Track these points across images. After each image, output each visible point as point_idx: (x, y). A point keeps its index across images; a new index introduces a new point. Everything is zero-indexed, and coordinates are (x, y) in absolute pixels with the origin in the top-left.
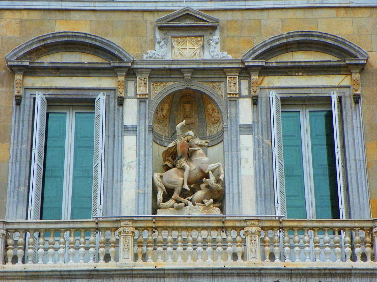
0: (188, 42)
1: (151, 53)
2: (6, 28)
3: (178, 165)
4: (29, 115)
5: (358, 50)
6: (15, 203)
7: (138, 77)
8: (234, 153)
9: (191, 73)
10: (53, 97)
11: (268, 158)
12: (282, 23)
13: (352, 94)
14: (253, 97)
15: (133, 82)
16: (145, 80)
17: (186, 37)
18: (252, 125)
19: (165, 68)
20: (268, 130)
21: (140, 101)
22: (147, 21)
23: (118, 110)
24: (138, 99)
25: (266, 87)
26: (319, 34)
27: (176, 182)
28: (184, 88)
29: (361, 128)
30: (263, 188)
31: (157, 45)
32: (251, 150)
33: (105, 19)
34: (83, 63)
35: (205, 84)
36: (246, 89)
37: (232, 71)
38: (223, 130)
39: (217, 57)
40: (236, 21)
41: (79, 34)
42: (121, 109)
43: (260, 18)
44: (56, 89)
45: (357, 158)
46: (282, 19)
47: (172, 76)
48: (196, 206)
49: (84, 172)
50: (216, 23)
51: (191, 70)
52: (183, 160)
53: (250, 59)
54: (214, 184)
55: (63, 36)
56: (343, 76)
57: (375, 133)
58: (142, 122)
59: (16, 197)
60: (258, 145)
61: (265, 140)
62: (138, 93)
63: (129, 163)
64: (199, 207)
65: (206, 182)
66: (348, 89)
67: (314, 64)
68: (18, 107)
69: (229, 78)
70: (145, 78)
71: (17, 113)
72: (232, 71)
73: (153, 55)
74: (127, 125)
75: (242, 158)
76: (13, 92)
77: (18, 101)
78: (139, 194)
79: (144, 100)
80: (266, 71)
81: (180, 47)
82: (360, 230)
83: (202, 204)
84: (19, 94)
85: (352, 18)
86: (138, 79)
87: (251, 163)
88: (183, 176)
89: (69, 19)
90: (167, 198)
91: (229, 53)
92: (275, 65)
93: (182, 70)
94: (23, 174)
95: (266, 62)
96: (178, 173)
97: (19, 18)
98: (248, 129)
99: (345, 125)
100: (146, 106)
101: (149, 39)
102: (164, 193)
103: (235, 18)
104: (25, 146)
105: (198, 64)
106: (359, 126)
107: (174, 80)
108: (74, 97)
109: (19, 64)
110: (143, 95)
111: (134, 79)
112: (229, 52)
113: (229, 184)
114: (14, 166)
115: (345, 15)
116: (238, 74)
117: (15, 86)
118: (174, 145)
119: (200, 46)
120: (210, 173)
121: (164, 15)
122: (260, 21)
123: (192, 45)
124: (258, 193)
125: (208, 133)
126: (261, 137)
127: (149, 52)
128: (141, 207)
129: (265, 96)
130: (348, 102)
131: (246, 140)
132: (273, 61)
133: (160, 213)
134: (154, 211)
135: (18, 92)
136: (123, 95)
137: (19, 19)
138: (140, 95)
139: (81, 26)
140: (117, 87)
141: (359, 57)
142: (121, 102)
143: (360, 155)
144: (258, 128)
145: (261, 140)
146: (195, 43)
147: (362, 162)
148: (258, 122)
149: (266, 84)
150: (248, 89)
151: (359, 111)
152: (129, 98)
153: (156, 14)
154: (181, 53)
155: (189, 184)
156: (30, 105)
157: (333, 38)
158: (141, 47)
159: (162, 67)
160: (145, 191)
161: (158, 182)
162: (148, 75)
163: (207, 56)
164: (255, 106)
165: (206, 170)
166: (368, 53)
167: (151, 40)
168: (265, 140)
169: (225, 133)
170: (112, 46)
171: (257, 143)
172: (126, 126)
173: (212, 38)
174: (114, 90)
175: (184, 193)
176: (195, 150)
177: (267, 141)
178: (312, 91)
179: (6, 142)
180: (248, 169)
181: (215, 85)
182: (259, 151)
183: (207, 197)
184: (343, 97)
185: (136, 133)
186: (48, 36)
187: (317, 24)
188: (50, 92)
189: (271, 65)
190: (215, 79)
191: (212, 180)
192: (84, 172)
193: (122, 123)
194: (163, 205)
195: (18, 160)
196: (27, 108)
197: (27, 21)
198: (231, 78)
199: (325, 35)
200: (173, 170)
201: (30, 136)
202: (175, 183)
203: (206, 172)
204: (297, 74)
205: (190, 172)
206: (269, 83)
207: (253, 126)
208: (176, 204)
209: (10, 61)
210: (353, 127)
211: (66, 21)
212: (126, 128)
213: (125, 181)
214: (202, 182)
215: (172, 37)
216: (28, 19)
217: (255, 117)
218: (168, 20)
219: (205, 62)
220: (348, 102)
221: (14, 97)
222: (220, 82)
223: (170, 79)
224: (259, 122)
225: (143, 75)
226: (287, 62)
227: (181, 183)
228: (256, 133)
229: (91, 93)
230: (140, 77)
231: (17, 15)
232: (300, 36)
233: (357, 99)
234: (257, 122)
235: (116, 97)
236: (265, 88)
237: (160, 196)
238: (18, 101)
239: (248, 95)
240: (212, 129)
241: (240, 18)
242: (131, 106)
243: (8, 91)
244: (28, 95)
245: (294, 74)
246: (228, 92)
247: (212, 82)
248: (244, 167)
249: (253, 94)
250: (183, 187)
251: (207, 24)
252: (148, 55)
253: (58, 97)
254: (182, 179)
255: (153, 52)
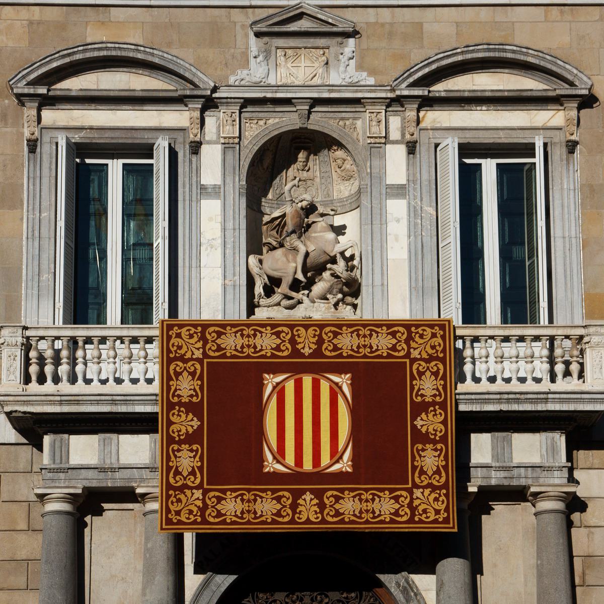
0: (303, 56)
1: (242, 74)
2: (7, 35)
3: (288, 244)
4: (50, 169)
5: (576, 75)
6: (35, 297)
7: (222, 111)
8: (376, 228)
9: (307, 105)
10: (88, 141)
11: (429, 234)
12: (457, 29)
13: (563, 140)
14: (408, 142)
15: (215, 118)
16: (233, 115)
17: (300, 48)
18: (405, 185)
19: (265, 97)
20: (430, 193)
21: (225, 147)
22: (235, 23)
23: (190, 161)
24: (222, 144)
25: (429, 128)
26: (515, 48)
27: (284, 269)
28: (297, 127)
29: (575, 190)
30: (420, 278)
31: (252, 61)
32: (405, 222)
33: (167, 20)
34: (134, 90)
35: (331, 122)
36: (397, 131)
37: (374, 102)
38: (359, 191)
39: (350, 80)
40: (383, 25)
41: (125, 46)
42: (194, 159)
43: (422, 21)
44: (91, 128)
45: (567, 235)
46: (456, 23)
47: (277, 109)
48: (316, 304)
49: (138, 252)
50: (349, 27)
51: (309, 100)
52: (294, 236)
53: (404, 85)
54: (345, 272)
55: (99, 49)
56: (551, 113)
57: (591, 193)
58: (229, 180)
59: (36, 289)
60: (415, 215)
61: (425, 208)
62: (222, 135)
63: (209, 240)
64: (322, 306)
65: (330, 269)
66: (557, 132)
67: (506, 94)
68: (31, 155)
69: (370, 112)
70: (232, 113)
71: (32, 165)
72: (374, 102)
73: (246, 76)
74: (204, 183)
75: (390, 234)
76: (23, 134)
77: (33, 146)
78: (225, 286)
79: (232, 146)
80: (428, 102)
81: (289, 65)
82: (565, 338)
83: (326, 301)
84: (33, 137)
85: (570, 22)
86: (221, 113)
87: (404, 241)
88: (296, 262)
89: (107, 20)
90: (269, 291)
91: (370, 75)
92: (445, 95)
93: (293, 101)
94: (44, 256)
95: (427, 88)
96: (286, 256)
97: (26, 19)
98: (399, 191)
99: (551, 187)
100: (234, 156)
101: (239, 51)
102: (265, 284)
103: (381, 21)
104: (46, 214)
105: (320, 92)
106: (572, 187)
107: (281, 114)
108: (120, 141)
109: (32, 91)
110: (230, 138)
111: (215, 113)
112: (372, 72)
113: (368, 272)
114: (30, 243)
115: (559, 18)
116: (384, 108)
117: (26, 125)
118: (280, 214)
119: (323, 63)
120: (338, 256)
121: (265, 13)
122: (421, 25)
123: (310, 62)
124: (413, 285)
125: (335, 194)
126: (419, 203)
127: (239, 72)
128: (229, 306)
129: (427, 141)
130: (558, 153)
131: (397, 208)
132: (440, 88)
133: (261, 314)
134: (251, 307)
135: (33, 134)
136: (197, 139)
137: (27, 20)
138: (225, 138)
139: (130, 35)
140: (188, 127)
141: (577, 84)
142: (196, 148)
143: (573, 230)
144: (415, 189)
145: (418, 208)
146: (314, 58)
147: (574, 241)
148: (414, 182)
149: (430, 123)
150: (400, 129)
151: (574, 165)
152: (209, 143)
153: (250, 10)
154: (292, 74)
155: (305, 272)
156: (51, 154)
157: (537, 56)
158: (226, 64)
159: (262, 96)
160: (234, 282)
161: (255, 270)
162: (238, 108)
163: (335, 78)
164: (412, 155)
165: (332, 252)
166: (591, 77)
167: (243, 53)
168: (426, 208)
169: (363, 197)
170: (180, 64)
171: (414, 213)
172: (203, 185)
173: (343, 50)
174: (182, 130)
175: (296, 285)
176: (314, 222)
177: (429, 208)
178: (501, 134)
179: (17, 209)
180: (398, 249)
181: (348, 123)
182: (416, 224)
183: (330, 291)
184: (549, 145)
185: (219, 195)
186: (76, 50)
187: (514, 31)
188: (82, 134)
189: (437, 95)
190: (348, 113)
191: (340, 267)
192: (138, 252)
193: (198, 181)
194: (264, 303)
195: (37, 234)
196: (45, 158)
197: (39, 23)
198: (373, 113)
199: (524, 50)
200: (279, 252)
201: (53, 199)
202: (282, 271)
203: (332, 254)
204: (478, 108)
205: (307, 254)
206: (434, 121)
207: (407, 186)
208: (285, 302)
209: (17, 87)
210: (562, 189)
211: (103, 23)
212: (203, 188)
213: (205, 267)
214: (325, 269)
215: (277, 48)
216: (41, 20)
217: (411, 172)
218: (271, 22)
219: (332, 87)
220: (558, 153)
221: (26, 142)
222: (355, 119)
223: (274, 114)
224: (416, 180)
225: (231, 108)
226: (464, 91)
227: (291, 271)
228: (412, 197)
229: (147, 135)
230: (224, 111)
231: (24, 12)
232: (485, 52)
233: (572, 146)
234: (414, 181)
235: (188, 141)
236: (427, 129)
237: (259, 289)
238: (33, 146)
239: (400, 139)
240: (342, 188)
241: (388, 20)
242: (211, 155)
243: (15, 132)
244: (46, 138)
245: (474, 108)
246: (368, 135)
247: (342, 119)
248: (392, 248)
249: (408, 137)
250: (296, 277)
251: (335, 29)
252: (238, 77)
253: (94, 141)
254: (294, 265)
255: (245, 72)
